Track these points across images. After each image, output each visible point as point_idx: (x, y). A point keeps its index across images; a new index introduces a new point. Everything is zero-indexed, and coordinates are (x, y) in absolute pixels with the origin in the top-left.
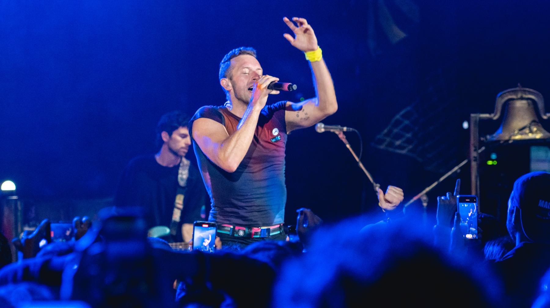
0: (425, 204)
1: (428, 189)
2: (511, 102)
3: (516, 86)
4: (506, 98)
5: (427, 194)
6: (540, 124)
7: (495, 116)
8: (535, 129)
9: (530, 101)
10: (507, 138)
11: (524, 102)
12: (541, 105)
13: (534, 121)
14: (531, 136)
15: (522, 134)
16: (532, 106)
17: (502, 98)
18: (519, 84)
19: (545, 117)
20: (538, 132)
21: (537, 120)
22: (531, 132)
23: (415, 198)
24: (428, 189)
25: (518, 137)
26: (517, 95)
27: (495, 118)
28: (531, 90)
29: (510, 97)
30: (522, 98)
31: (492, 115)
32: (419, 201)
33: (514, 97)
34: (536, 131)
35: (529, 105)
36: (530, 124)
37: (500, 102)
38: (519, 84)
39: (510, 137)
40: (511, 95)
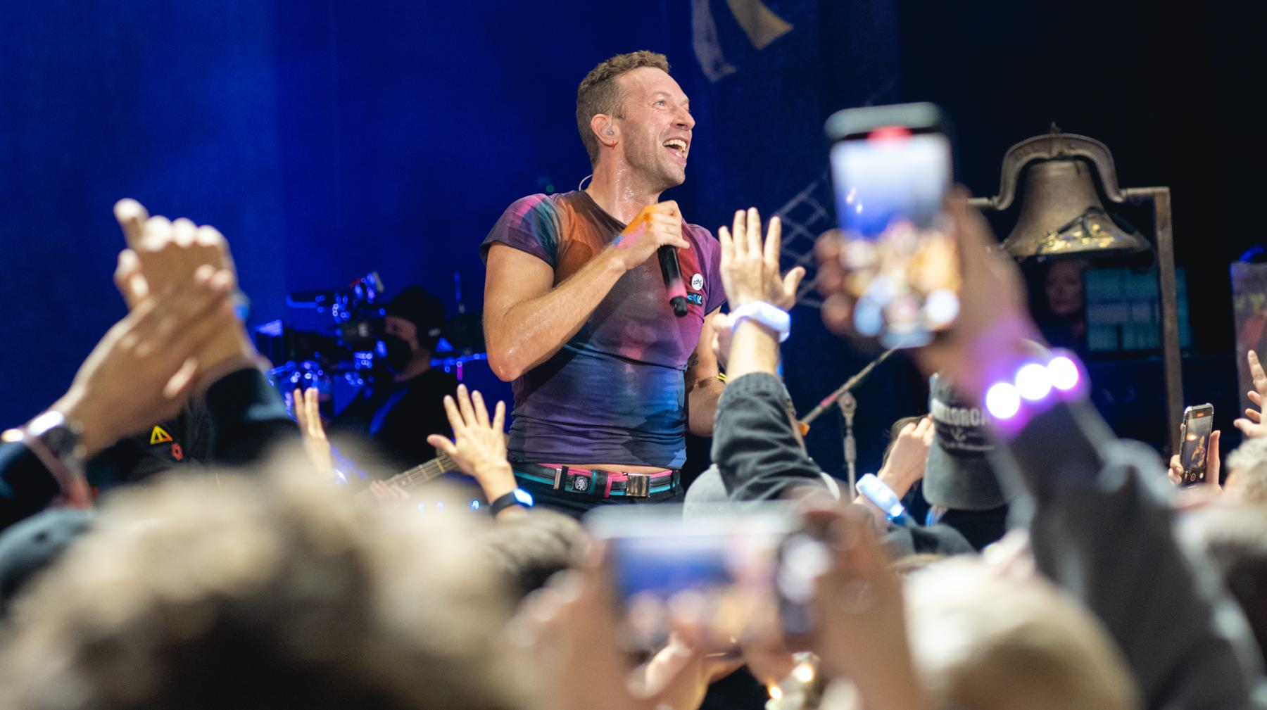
0: (849, 417)
1: (853, 381)
2: (1038, 166)
3: (1047, 131)
4: (1026, 159)
5: (854, 391)
6: (1107, 216)
7: (1001, 201)
8: (1096, 227)
9: (1081, 164)
10: (1032, 250)
11: (1067, 164)
12: (1106, 169)
13: (1092, 209)
14: (1086, 244)
15: (1068, 239)
16: (1085, 175)
17: (1017, 159)
18: (1053, 125)
19: (1118, 199)
20: (1103, 233)
21: (1100, 205)
22: (1087, 234)
23: (826, 403)
24: (853, 381)
25: (1058, 246)
26: (1050, 152)
27: (1003, 206)
28: (1083, 137)
29: (1033, 156)
30: (1062, 158)
31: (996, 200)
32: (835, 408)
33: (1044, 155)
34: (1098, 231)
35: (1078, 171)
36: (1084, 216)
37: (1011, 168)
38: (1053, 125)
39: (1040, 248)
40: (1037, 151)
